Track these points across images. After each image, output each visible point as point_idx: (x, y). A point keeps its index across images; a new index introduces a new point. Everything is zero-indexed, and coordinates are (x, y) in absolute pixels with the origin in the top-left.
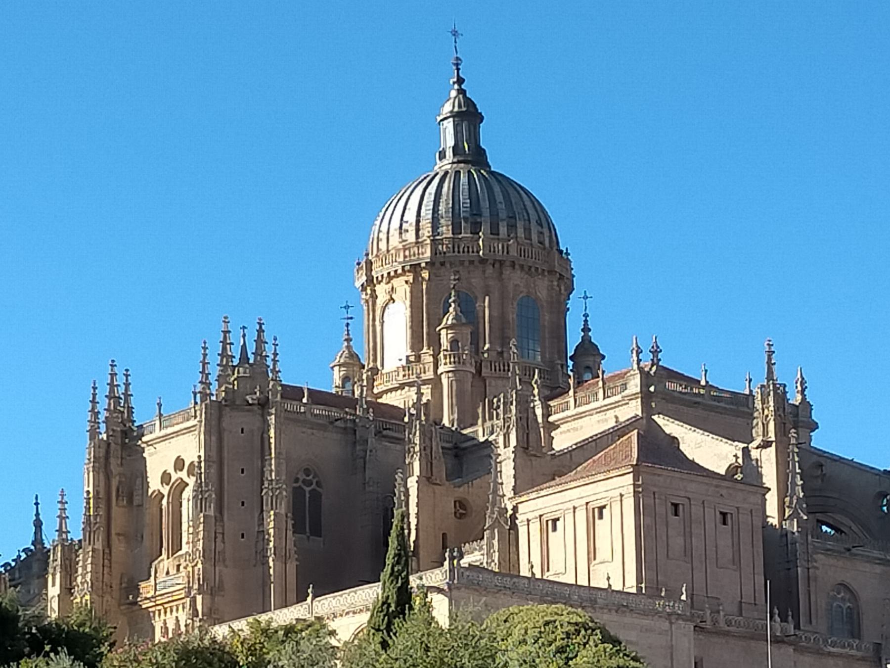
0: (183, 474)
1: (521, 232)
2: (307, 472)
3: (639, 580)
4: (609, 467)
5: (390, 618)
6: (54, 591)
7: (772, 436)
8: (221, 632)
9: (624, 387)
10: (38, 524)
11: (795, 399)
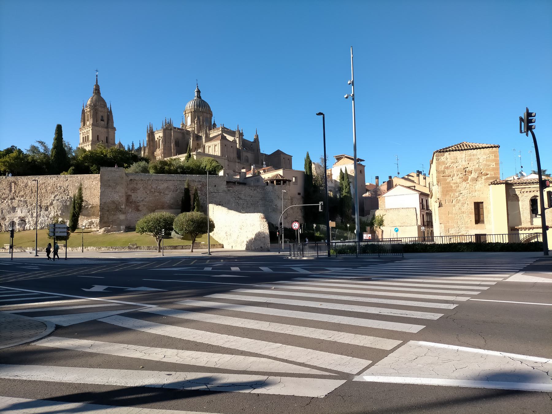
0: (160, 138)
1: (206, 108)
2: (177, 138)
3: (221, 154)
4: (217, 140)
5: (188, 158)
6: (142, 153)
7: (238, 137)
8: (166, 159)
9: (219, 129)
10: (140, 144)
11: (241, 132)
